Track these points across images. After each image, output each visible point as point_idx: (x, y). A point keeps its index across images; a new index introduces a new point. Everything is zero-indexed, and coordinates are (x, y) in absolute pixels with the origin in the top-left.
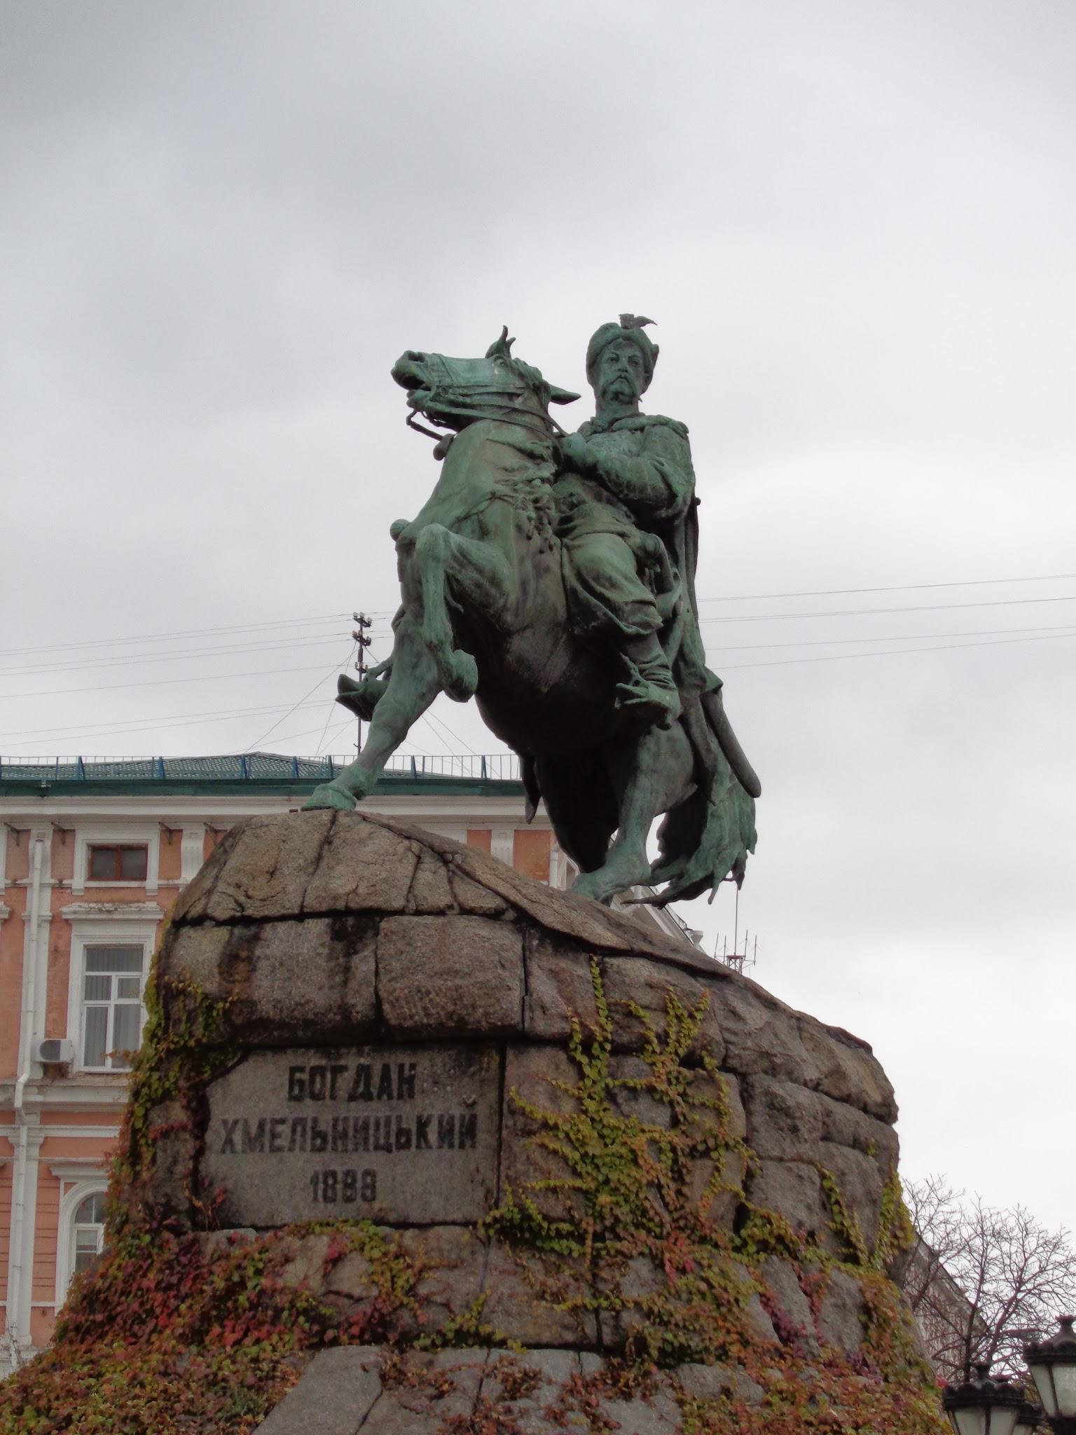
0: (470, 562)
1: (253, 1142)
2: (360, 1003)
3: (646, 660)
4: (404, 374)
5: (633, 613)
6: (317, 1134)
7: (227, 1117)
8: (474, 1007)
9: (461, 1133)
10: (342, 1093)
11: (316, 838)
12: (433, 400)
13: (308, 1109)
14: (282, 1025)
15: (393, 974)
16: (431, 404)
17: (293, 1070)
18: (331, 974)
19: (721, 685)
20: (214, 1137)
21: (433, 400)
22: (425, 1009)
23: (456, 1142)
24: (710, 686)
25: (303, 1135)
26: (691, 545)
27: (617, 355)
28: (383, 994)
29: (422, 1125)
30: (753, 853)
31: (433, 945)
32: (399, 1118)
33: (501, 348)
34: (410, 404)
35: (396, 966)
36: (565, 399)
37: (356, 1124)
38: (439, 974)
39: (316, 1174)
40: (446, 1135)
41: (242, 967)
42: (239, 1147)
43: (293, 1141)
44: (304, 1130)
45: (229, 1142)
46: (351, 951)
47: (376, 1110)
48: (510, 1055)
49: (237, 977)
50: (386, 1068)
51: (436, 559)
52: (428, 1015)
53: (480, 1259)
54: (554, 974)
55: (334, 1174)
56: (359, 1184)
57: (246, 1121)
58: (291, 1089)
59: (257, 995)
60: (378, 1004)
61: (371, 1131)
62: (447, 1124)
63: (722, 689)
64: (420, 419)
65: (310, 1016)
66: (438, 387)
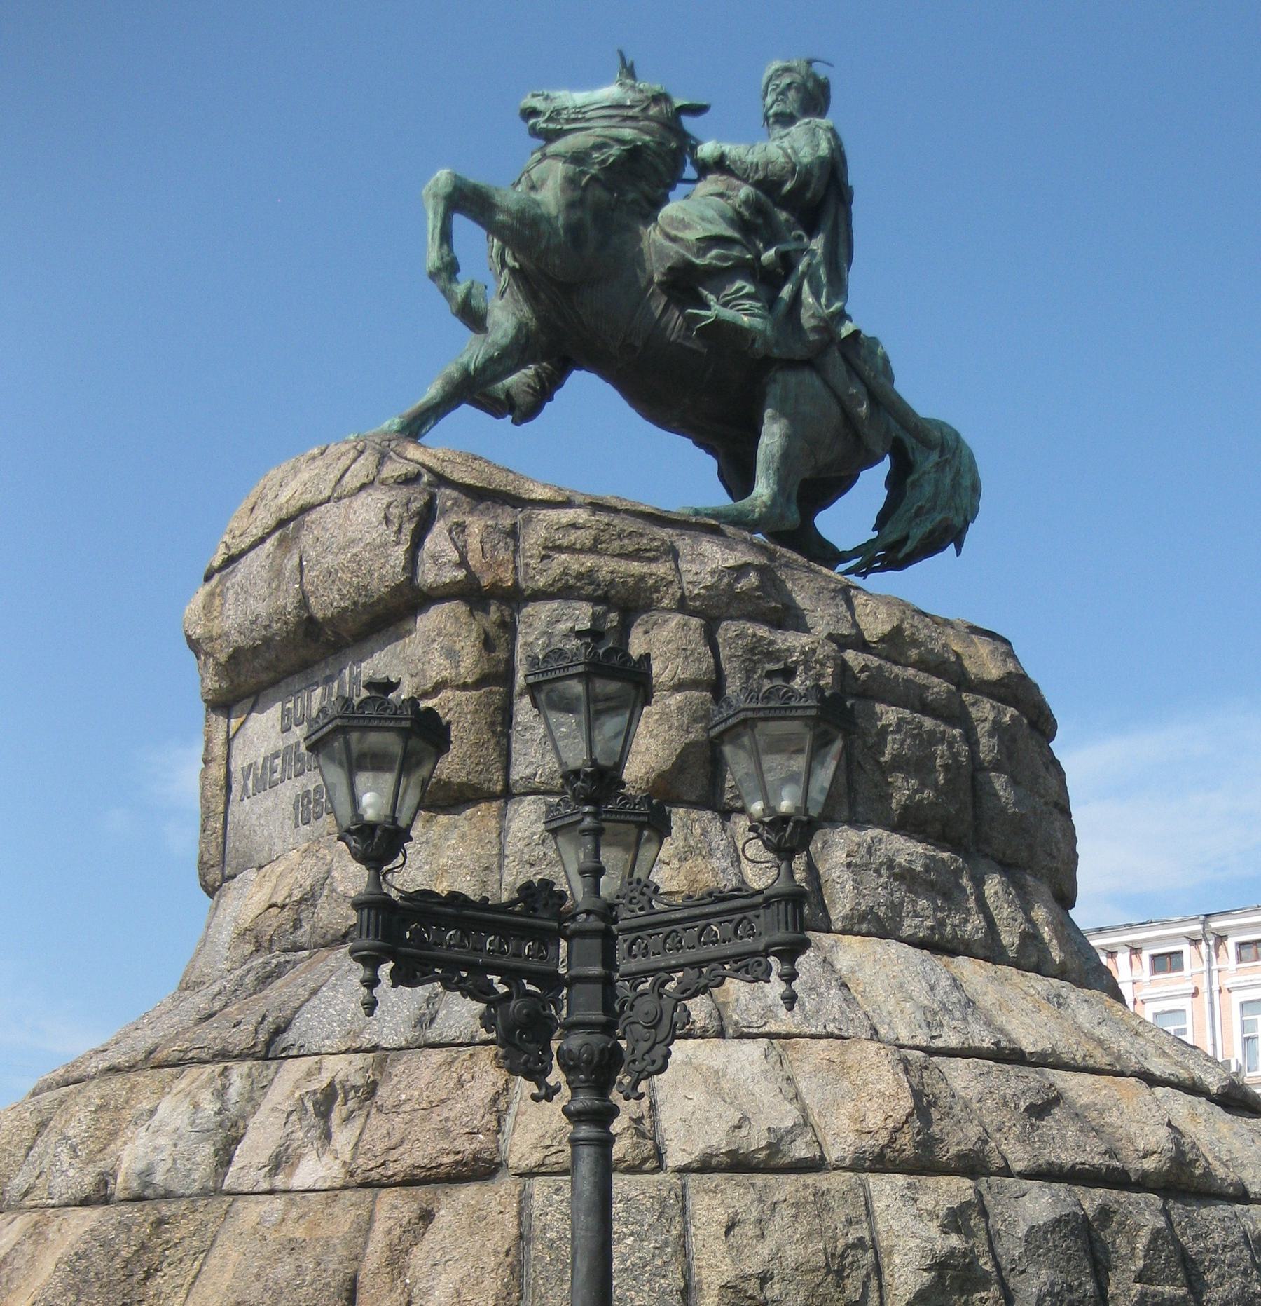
2: (288, 601)
5: (709, 249)
8: (371, 574)
35: (313, 553)
36: (697, 110)
38: (342, 549)
41: (217, 602)
49: (215, 614)
52: (342, 597)
65: (264, 632)
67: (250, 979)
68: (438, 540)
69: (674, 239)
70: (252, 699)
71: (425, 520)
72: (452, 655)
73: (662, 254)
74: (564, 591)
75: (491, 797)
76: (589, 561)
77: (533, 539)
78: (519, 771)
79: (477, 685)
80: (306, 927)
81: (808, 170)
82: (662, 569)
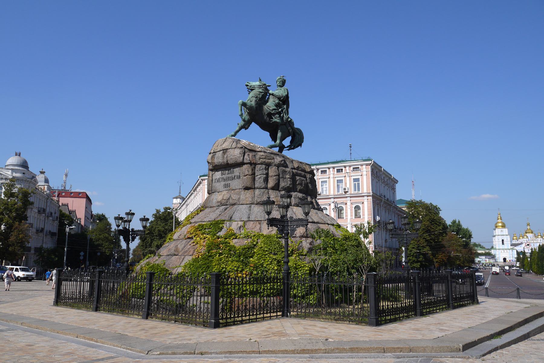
1: (218, 181)
2: (225, 161)
6: (224, 179)
10: (227, 174)
11: (224, 141)
14: (219, 165)
18: (222, 158)
20: (214, 181)
29: (235, 176)
33: (260, 80)
34: (247, 88)
41: (213, 158)
46: (225, 154)
47: (230, 175)
54: (249, 155)
59: (215, 162)
60: (227, 161)
67: (223, 209)
68: (246, 156)
69: (269, 109)
71: (244, 153)
72: (248, 171)
73: (267, 111)
74: (261, 164)
75: (253, 189)
76: (265, 160)
77: (257, 157)
78: (256, 186)
79: (251, 175)
80: (228, 202)
81: (284, 97)
82: (273, 161)
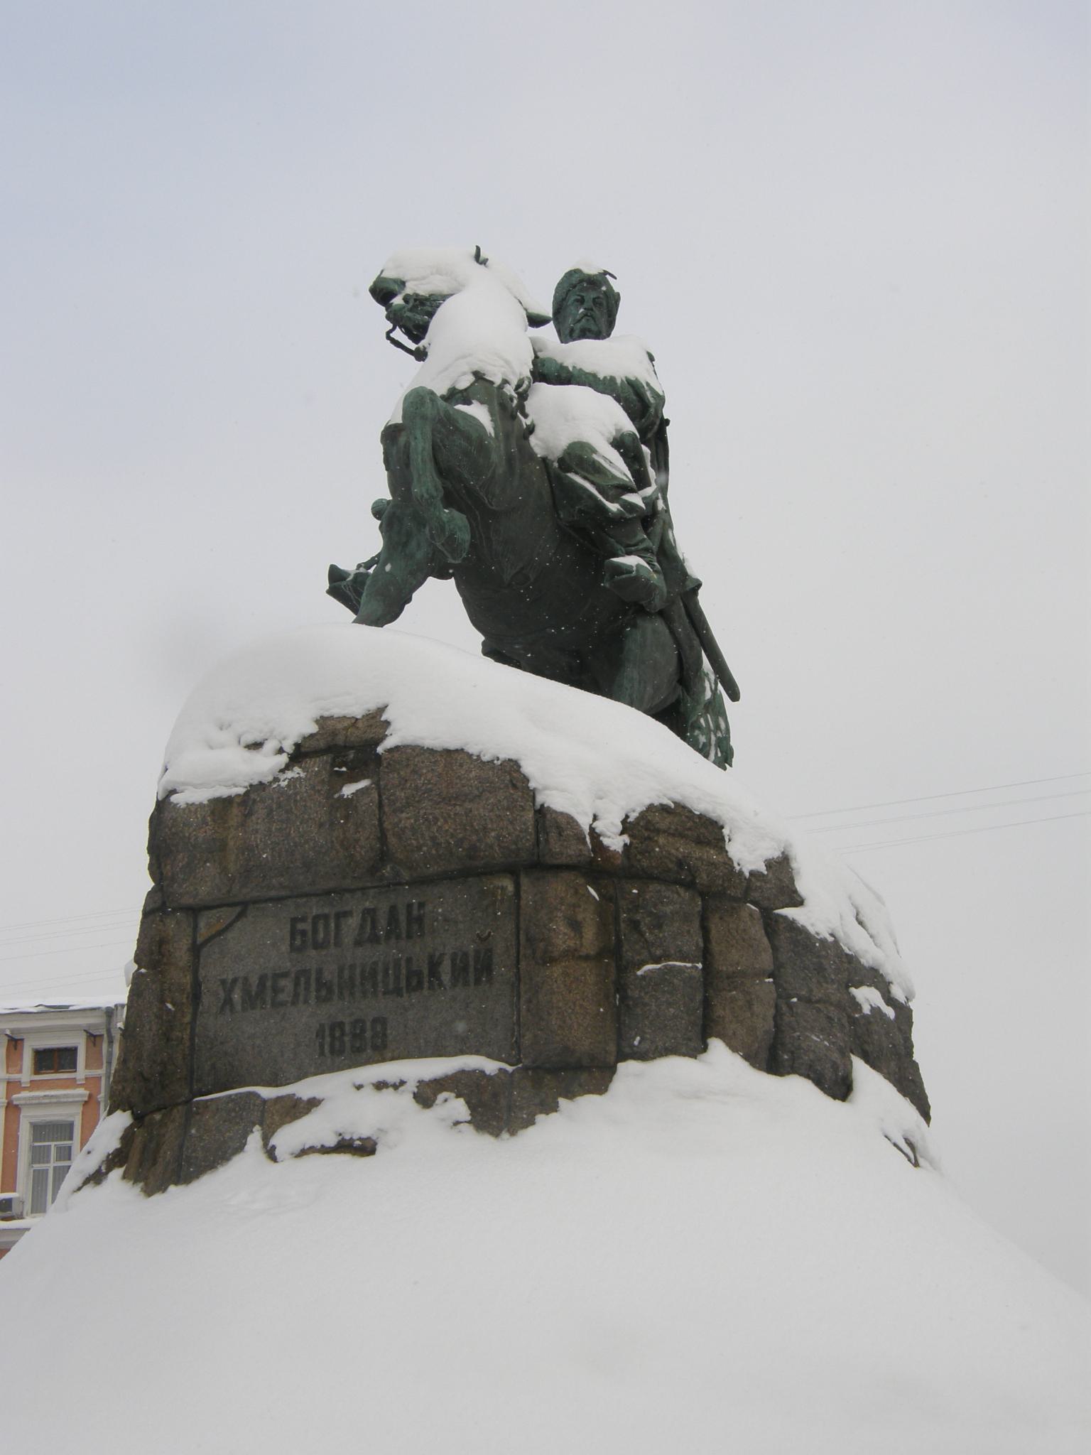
0: (457, 429)
1: (252, 1000)
3: (633, 542)
4: (382, 290)
6: (320, 984)
7: (224, 977)
9: (476, 969)
12: (411, 310)
13: (312, 959)
15: (398, 804)
16: (409, 314)
17: (294, 921)
19: (699, 585)
21: (411, 310)
22: (433, 839)
23: (471, 978)
24: (690, 585)
25: (307, 989)
26: (662, 464)
27: (583, 297)
28: (386, 825)
30: (731, 766)
31: (440, 770)
32: (409, 960)
37: (363, 972)
39: (322, 1026)
40: (460, 972)
42: (239, 1008)
43: (296, 995)
44: (308, 983)
45: (228, 1001)
48: (525, 881)
50: (393, 910)
51: (424, 418)
53: (503, 1102)
55: (341, 1025)
56: (368, 1034)
57: (246, 979)
58: (293, 938)
61: (380, 977)
62: (461, 961)
63: (700, 591)
64: (399, 335)
66: (415, 300)
70: (238, 909)
72: (575, 926)
